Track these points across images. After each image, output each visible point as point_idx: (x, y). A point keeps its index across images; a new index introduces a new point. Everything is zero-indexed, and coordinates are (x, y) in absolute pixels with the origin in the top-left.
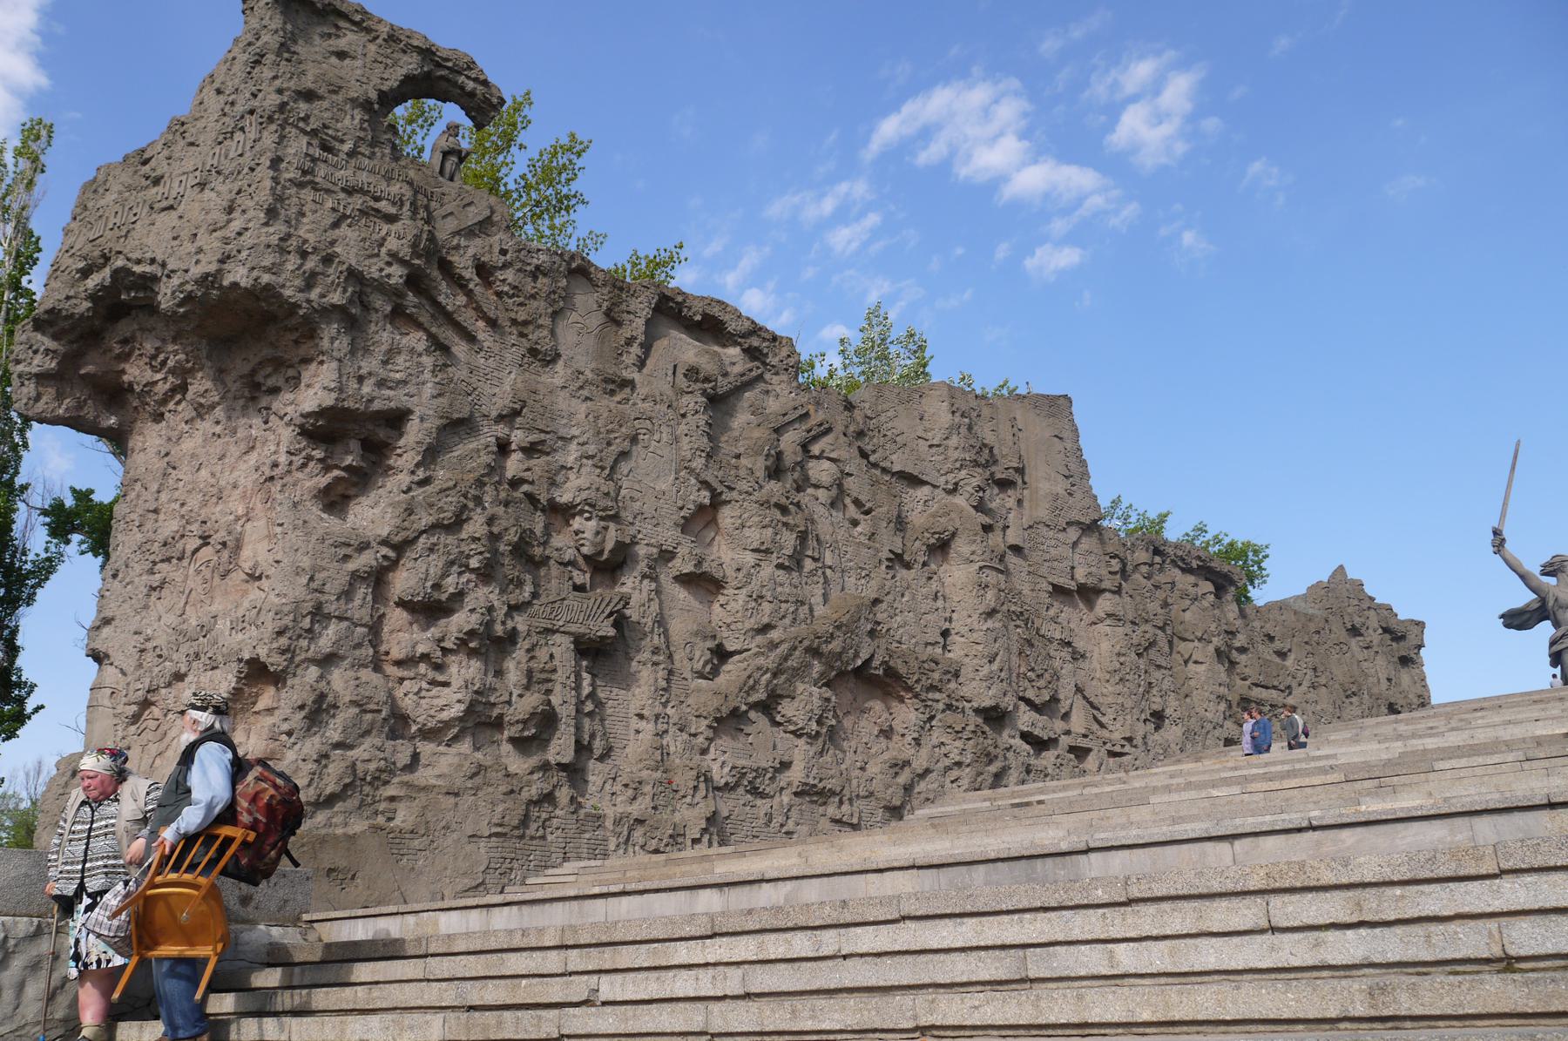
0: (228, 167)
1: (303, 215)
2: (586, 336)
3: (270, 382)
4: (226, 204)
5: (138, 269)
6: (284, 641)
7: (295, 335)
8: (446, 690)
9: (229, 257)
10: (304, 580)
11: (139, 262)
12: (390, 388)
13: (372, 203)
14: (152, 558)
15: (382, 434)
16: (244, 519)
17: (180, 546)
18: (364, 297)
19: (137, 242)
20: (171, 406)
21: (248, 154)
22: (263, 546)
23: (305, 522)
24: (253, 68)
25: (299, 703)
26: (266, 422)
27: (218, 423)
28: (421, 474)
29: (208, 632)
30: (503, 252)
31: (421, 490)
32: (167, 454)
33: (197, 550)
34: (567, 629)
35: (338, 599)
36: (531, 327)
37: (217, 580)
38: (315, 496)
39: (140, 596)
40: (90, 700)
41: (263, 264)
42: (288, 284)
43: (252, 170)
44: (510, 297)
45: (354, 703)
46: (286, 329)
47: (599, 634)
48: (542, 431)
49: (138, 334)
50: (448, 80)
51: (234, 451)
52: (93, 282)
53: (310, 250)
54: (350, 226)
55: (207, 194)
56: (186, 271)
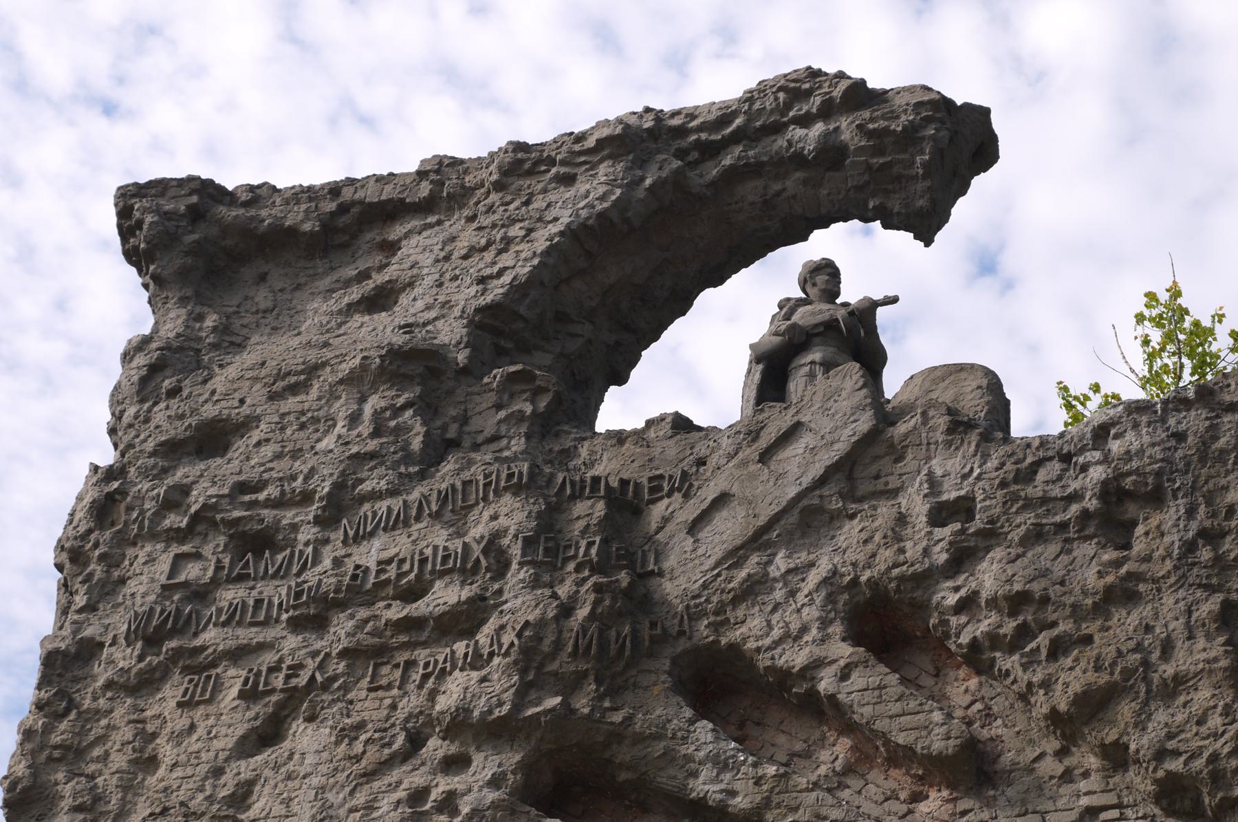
1: (151, 763)
36: (1126, 710)
54: (311, 719)
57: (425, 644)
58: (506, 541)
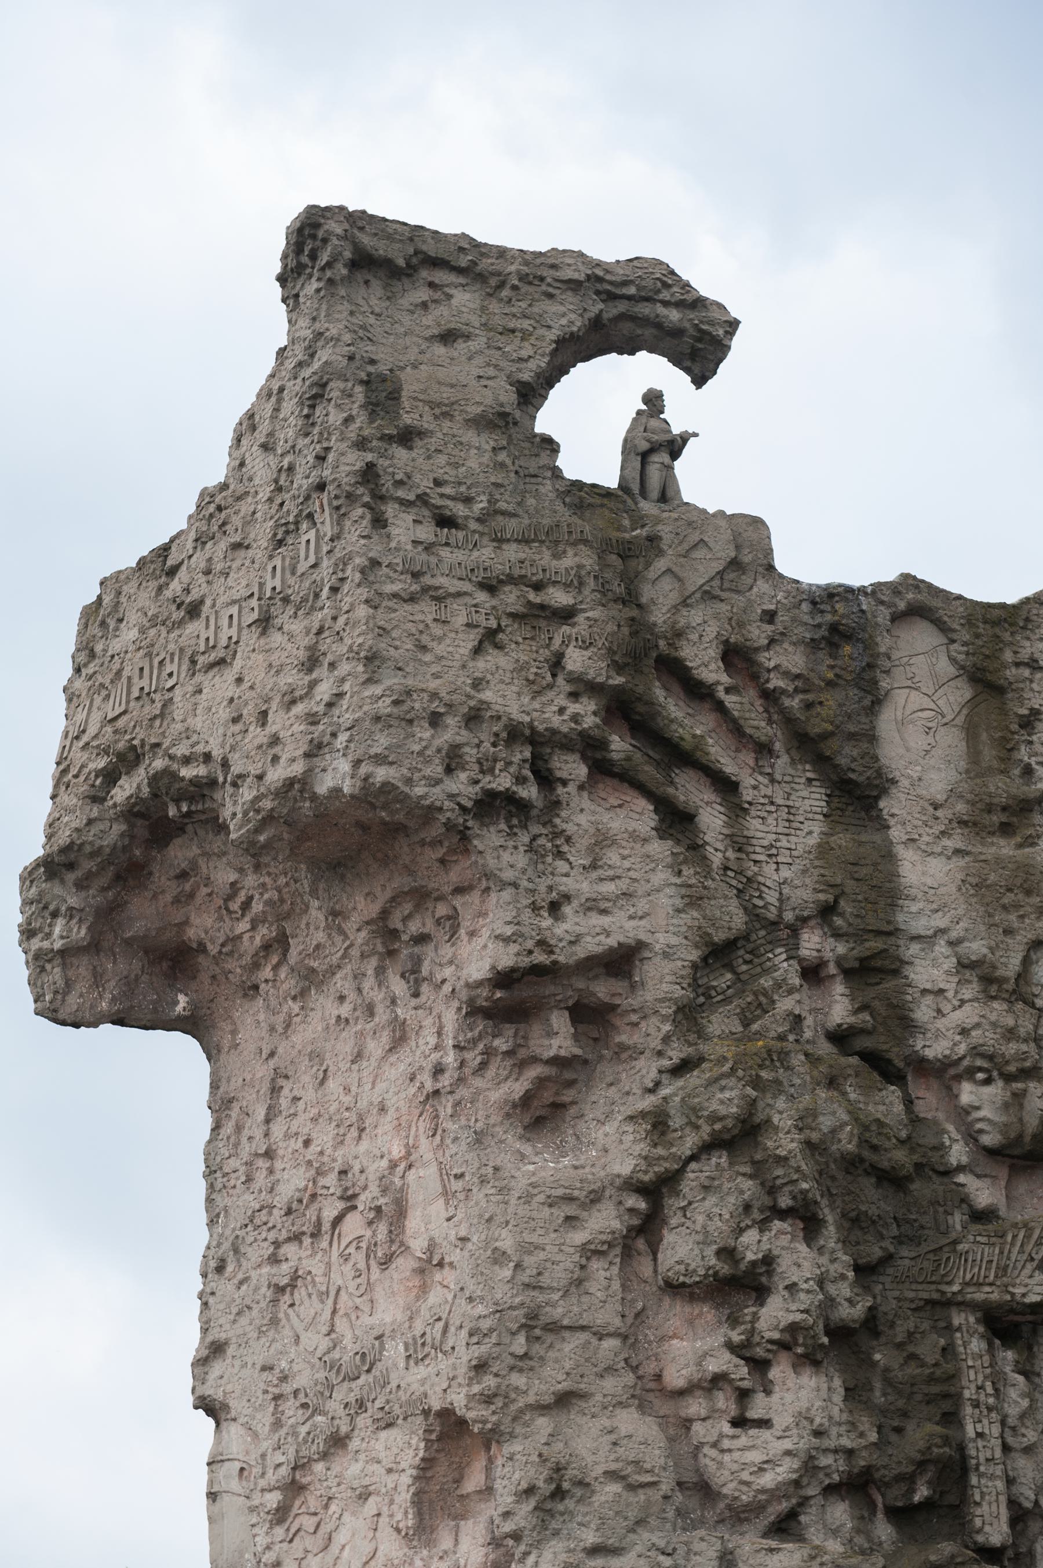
0: (298, 589)
2: (942, 731)
3: (414, 927)
4: (302, 654)
5: (187, 772)
6: (489, 1381)
7: (440, 852)
8: (766, 1434)
9: (320, 746)
10: (507, 1273)
11: (187, 760)
12: (604, 912)
13: (532, 596)
14: (272, 1236)
15: (603, 990)
16: (403, 1166)
17: (311, 1214)
18: (540, 763)
19: (179, 727)
20: (267, 973)
21: (325, 563)
22: (438, 1208)
23: (496, 1169)
24: (313, 407)
25: (524, 1485)
26: (416, 995)
27: (342, 998)
28: (676, 1053)
29: (372, 1365)
30: (769, 617)
31: (680, 1083)
32: (272, 1054)
33: (338, 1221)
35: (566, 1294)
37: (375, 1273)
38: (508, 1115)
39: (263, 1304)
40: (211, 1482)
41: (373, 751)
42: (417, 776)
43: (335, 590)
44: (791, 696)
45: (612, 1475)
46: (423, 843)
48: (879, 933)
49: (202, 862)
50: (633, 318)
51: (375, 1048)
52: (123, 791)
53: (442, 710)
55: (276, 638)
56: (260, 777)
57: (545, 618)
58: (583, 573)
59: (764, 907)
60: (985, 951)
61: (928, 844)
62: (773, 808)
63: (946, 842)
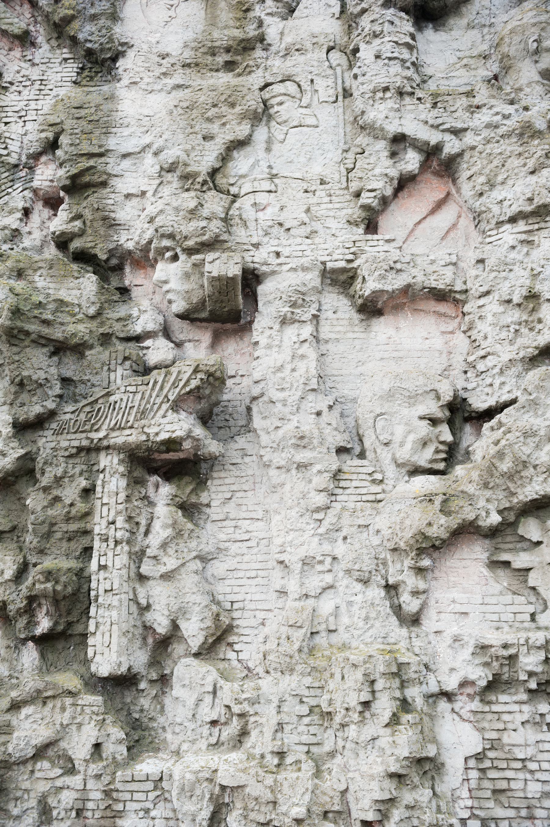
34: (112, 442)
47: (164, 436)
59: (8, 155)
60: (179, 153)
61: (148, 84)
62: (28, 83)
63: (170, 82)
